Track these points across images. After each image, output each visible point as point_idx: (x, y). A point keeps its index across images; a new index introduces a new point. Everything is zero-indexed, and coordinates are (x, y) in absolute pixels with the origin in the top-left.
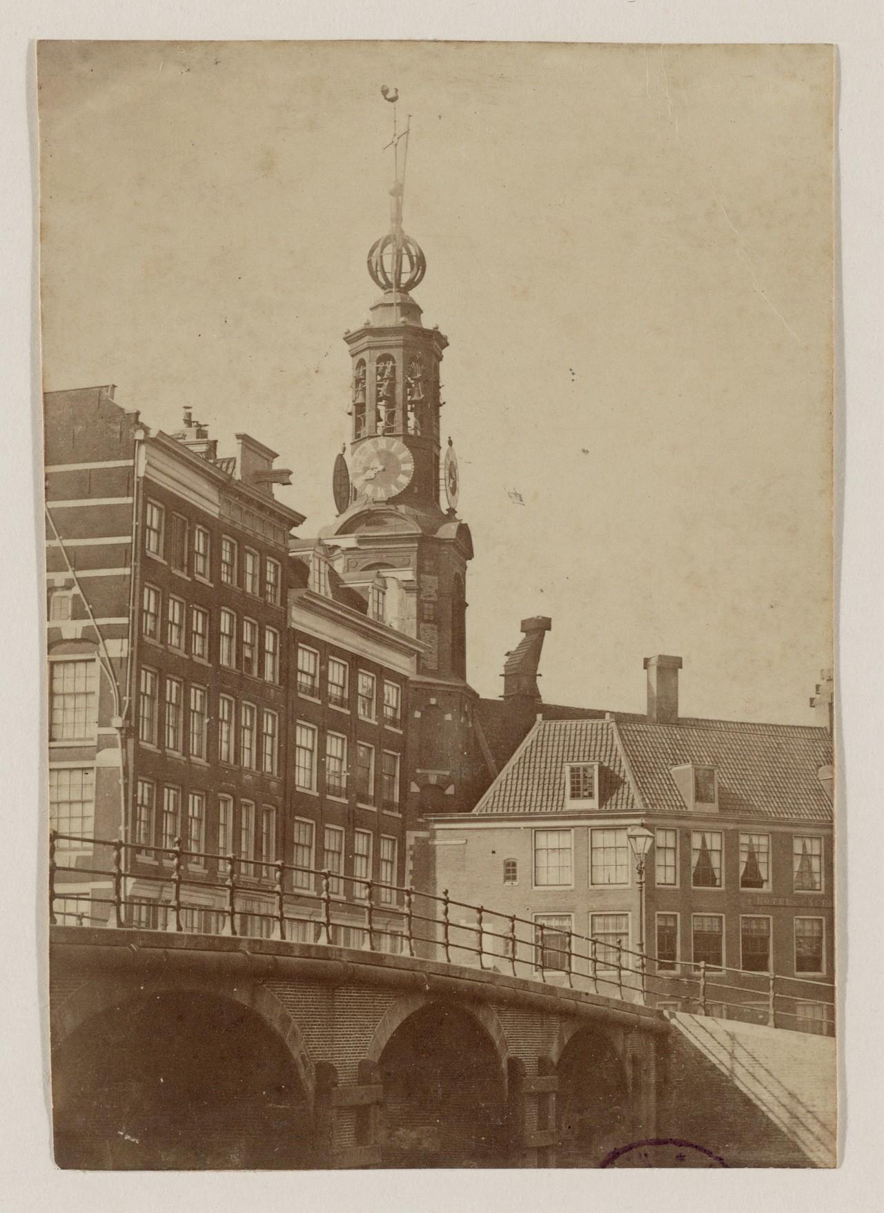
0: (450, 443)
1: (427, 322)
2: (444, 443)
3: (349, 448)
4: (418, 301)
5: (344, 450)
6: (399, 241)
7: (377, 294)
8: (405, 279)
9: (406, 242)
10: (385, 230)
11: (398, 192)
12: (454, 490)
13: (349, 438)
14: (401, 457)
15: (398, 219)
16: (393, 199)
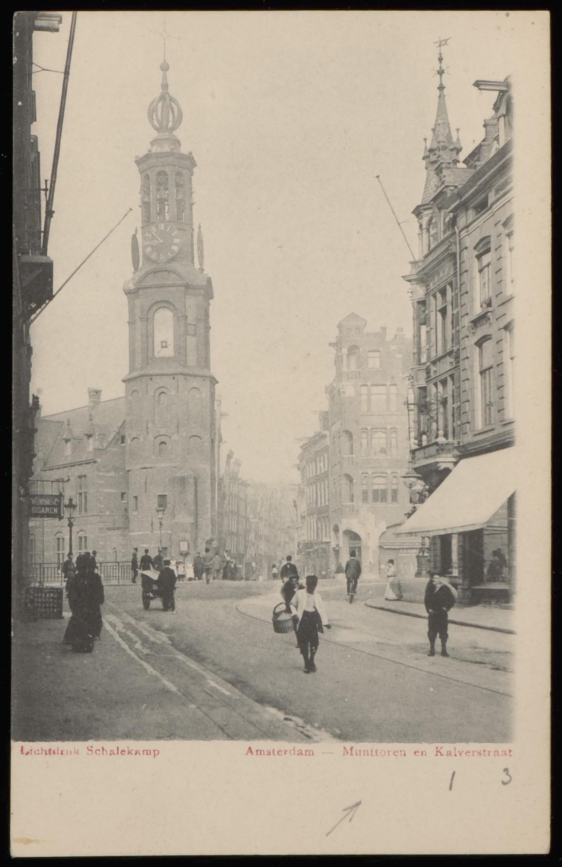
0: (200, 227)
1: (184, 150)
2: (196, 227)
3: (140, 231)
4: (179, 138)
5: (136, 231)
6: (165, 98)
7: (155, 134)
8: (170, 124)
9: (172, 99)
10: (158, 92)
11: (165, 68)
12: (201, 257)
13: (139, 225)
14: (173, 234)
15: (165, 86)
16: (162, 73)
